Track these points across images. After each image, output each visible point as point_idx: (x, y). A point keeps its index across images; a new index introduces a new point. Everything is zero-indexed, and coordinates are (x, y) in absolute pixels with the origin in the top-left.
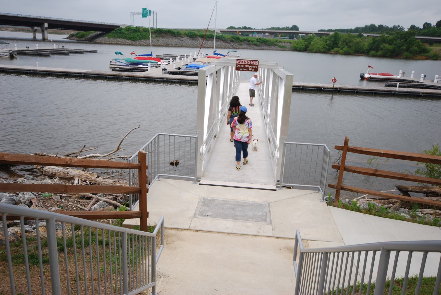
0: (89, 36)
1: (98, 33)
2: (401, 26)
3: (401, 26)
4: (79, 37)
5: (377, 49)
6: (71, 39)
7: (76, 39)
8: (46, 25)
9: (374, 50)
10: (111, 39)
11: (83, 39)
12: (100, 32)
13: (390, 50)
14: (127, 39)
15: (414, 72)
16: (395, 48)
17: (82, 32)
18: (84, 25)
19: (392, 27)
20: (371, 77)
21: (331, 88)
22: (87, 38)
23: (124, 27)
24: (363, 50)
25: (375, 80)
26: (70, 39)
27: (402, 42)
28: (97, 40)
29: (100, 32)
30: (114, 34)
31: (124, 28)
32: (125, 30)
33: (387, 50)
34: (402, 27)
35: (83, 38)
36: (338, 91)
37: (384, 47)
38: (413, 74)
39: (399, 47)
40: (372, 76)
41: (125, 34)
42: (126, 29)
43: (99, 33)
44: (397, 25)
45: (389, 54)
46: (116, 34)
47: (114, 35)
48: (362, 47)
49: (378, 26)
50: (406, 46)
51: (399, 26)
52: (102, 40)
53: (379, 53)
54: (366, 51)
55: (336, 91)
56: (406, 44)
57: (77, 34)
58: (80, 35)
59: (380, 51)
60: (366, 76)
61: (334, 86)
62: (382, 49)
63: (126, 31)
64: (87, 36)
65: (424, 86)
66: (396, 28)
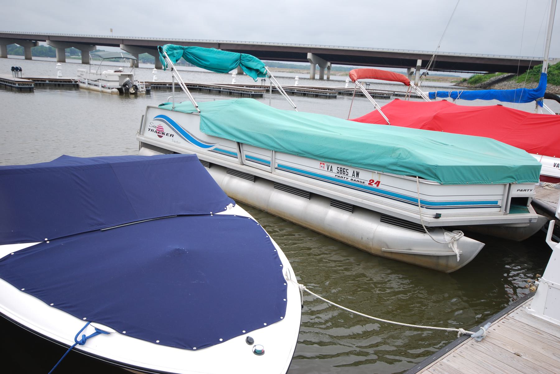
0: (488, 81)
1: (505, 76)
4: (471, 83)
6: (460, 86)
7: (466, 85)
8: (419, 63)
10: (520, 84)
11: (478, 85)
12: (509, 74)
14: (554, 84)
17: (480, 74)
18: (478, 62)
22: (484, 84)
23: (555, 63)
26: (458, 86)
28: (497, 85)
29: (509, 74)
30: (530, 76)
31: (554, 65)
32: (554, 68)
35: (478, 84)
41: (553, 75)
42: (557, 67)
43: (506, 75)
46: (535, 75)
47: (530, 78)
52: (505, 85)
57: (471, 78)
58: (473, 79)
63: (557, 69)
64: (484, 81)
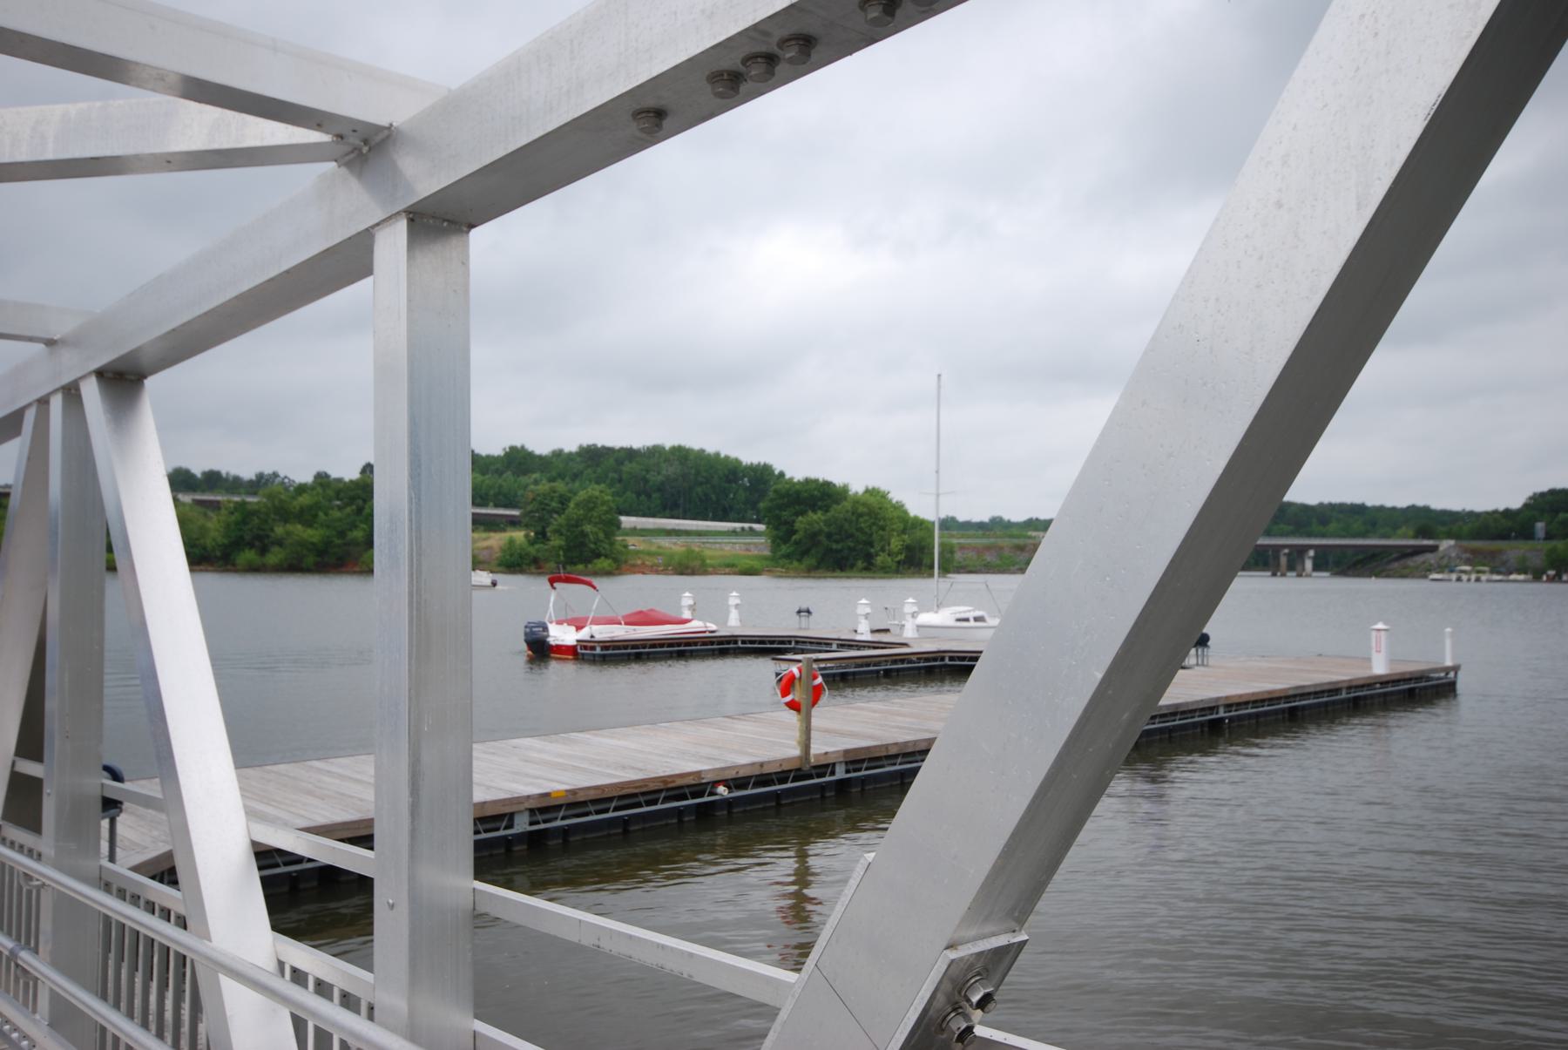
2: (282, 475)
3: (282, 475)
5: (262, 543)
9: (251, 546)
13: (313, 544)
15: (694, 598)
16: (328, 537)
19: (254, 478)
20: (598, 637)
21: (782, 777)
24: (205, 548)
25: (713, 650)
27: (349, 515)
33: (302, 544)
34: (286, 477)
36: (841, 782)
37: (288, 534)
38: (737, 606)
39: (342, 534)
40: (603, 632)
44: (268, 471)
45: (310, 560)
48: (197, 539)
49: (204, 474)
50: (364, 530)
51: (275, 475)
53: (276, 555)
54: (218, 554)
55: (822, 788)
56: (361, 522)
59: (276, 549)
60: (562, 635)
61: (806, 746)
62: (280, 543)
65: (943, 659)
66: (267, 480)
